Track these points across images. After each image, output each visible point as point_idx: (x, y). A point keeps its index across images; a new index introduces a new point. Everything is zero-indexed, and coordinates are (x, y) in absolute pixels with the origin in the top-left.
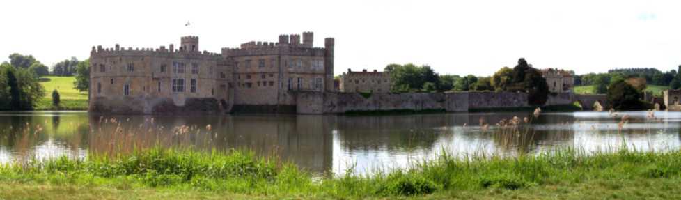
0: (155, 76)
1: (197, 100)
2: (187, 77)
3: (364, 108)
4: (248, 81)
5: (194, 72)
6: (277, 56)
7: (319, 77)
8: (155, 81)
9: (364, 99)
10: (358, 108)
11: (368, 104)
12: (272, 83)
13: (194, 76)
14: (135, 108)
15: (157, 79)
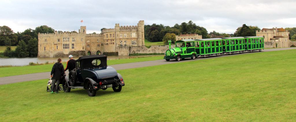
0: (55, 43)
1: (74, 52)
2: (70, 43)
3: (148, 53)
4: (107, 43)
5: (73, 41)
6: (115, 32)
7: (134, 40)
8: (55, 45)
9: (147, 49)
10: (145, 52)
11: (150, 51)
12: (113, 43)
13: (73, 43)
14: (47, 55)
15: (56, 44)
